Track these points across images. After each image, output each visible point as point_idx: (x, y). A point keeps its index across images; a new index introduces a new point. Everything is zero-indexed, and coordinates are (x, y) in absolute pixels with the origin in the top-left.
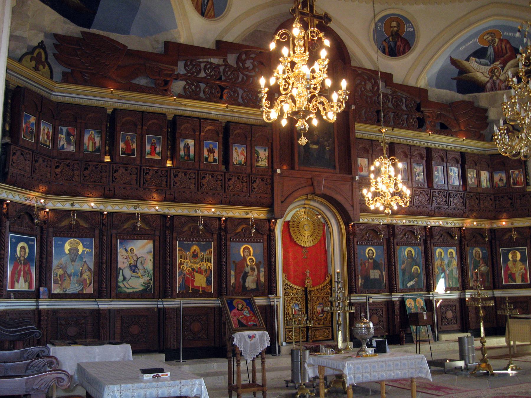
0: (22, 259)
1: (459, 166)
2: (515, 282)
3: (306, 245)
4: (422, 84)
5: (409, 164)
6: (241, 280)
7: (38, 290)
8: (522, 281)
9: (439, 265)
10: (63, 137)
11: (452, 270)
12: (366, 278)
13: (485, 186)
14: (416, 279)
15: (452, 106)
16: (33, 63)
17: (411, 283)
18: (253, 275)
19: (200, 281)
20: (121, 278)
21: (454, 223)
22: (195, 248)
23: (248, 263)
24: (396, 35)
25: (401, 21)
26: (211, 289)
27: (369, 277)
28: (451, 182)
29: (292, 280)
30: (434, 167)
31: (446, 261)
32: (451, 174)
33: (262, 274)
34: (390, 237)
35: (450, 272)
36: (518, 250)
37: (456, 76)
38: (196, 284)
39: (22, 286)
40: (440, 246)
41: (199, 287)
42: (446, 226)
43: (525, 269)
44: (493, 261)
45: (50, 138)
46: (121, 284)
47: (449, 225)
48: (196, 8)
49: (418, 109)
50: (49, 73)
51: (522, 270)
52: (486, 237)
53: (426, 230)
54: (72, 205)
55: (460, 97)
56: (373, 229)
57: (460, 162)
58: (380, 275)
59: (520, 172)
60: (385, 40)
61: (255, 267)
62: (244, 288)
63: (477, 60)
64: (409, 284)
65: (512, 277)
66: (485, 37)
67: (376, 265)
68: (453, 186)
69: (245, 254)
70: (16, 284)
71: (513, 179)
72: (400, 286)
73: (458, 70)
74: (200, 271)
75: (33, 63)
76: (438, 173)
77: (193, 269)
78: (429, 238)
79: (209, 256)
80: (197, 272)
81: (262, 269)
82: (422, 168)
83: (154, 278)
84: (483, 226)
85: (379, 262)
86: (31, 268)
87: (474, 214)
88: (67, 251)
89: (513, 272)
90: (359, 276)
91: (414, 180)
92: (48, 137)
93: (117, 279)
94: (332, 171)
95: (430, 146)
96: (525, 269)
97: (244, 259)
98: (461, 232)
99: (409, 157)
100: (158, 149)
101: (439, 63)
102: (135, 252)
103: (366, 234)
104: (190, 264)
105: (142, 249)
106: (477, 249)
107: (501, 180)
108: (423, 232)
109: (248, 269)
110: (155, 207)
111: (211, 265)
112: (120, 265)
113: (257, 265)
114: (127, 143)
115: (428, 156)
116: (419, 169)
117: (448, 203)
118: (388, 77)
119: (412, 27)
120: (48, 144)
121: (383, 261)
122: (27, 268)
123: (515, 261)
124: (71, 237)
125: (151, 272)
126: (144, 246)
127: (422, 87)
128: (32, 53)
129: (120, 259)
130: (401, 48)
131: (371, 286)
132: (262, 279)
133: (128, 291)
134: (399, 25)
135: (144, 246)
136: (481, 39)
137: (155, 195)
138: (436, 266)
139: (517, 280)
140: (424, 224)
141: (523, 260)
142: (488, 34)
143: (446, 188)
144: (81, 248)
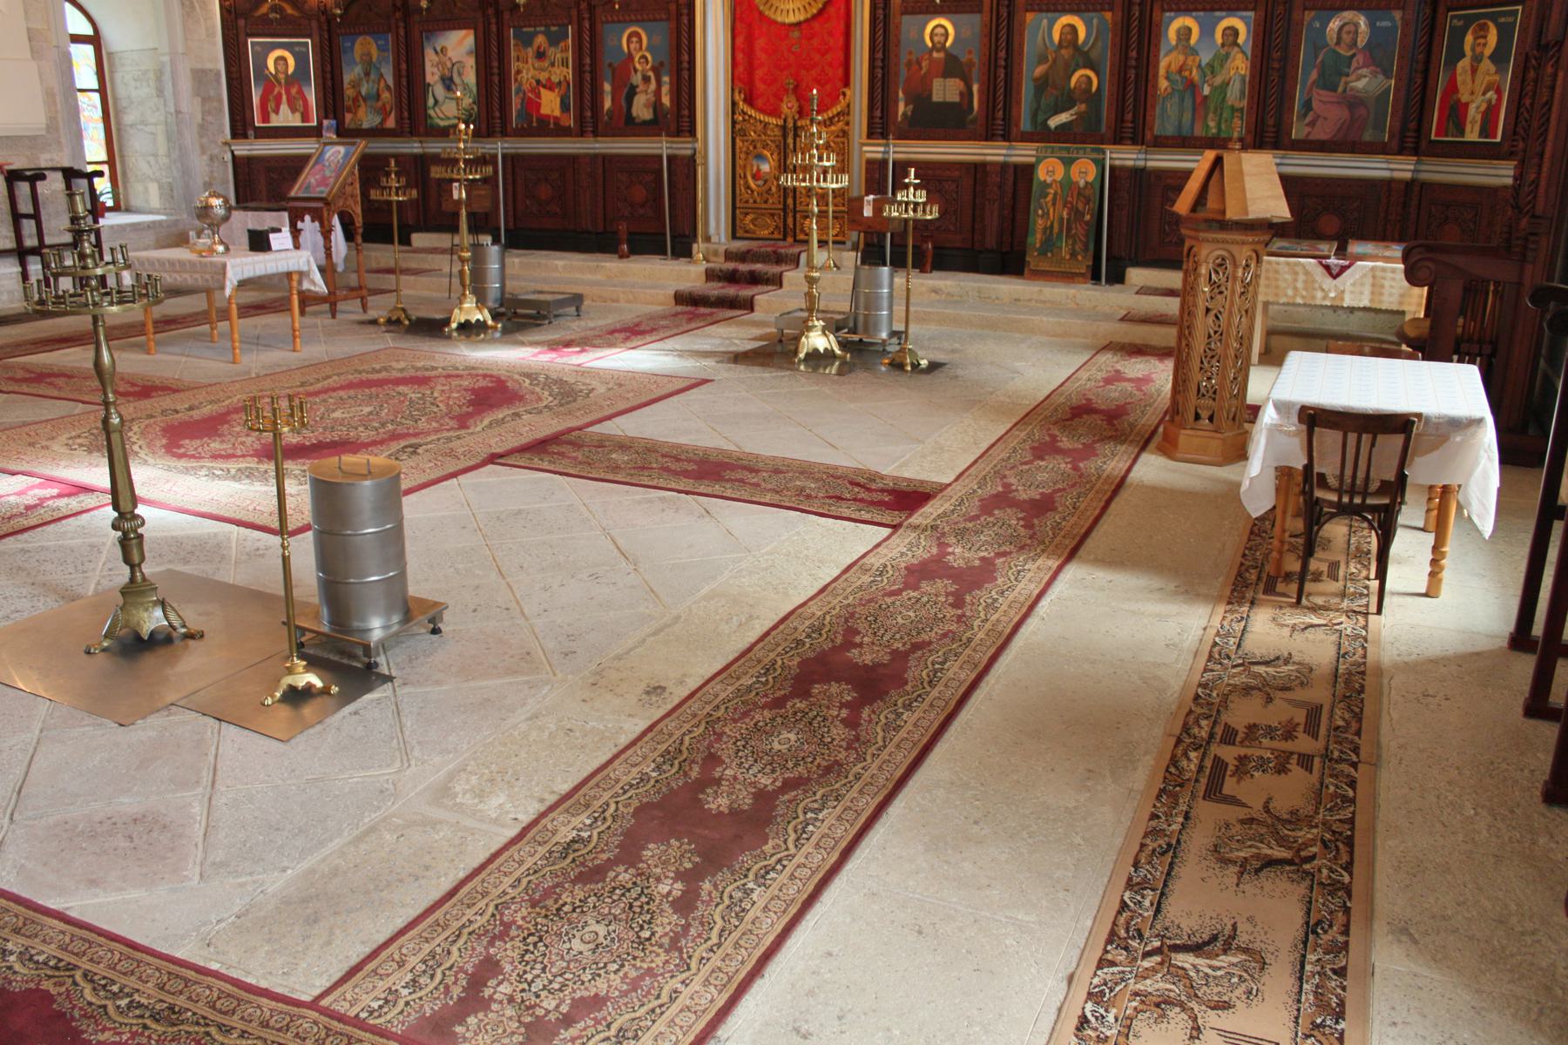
2: (1462, 134)
3: (791, 19)
6: (623, 103)
7: (320, 123)
8: (1483, 133)
9: (1174, 67)
12: (920, 99)
17: (1063, 118)
19: (550, 104)
20: (431, 102)
22: (540, 40)
29: (760, 102)
33: (665, 89)
38: (545, 110)
39: (285, 117)
41: (548, 116)
43: (1499, 92)
46: (431, 112)
51: (1489, 94)
58: (961, 94)
61: (651, 74)
62: (630, 119)
64: (1053, 122)
70: (273, 116)
72: (1025, 125)
74: (550, 86)
77: (538, 82)
80: (545, 87)
81: (666, 79)
83: (477, 102)
85: (964, 58)
88: (358, 59)
89: (1465, 98)
90: (901, 94)
96: (1499, 92)
97: (630, 57)
102: (450, 54)
104: (532, 72)
109: (637, 79)
112: (429, 79)
121: (974, 56)
122: (294, 91)
123: (1477, 59)
124: (360, 34)
125: (475, 89)
126: (461, 42)
129: (429, 68)
132: (666, 100)
133: (442, 124)
135: (461, 42)
138: (1162, 72)
139: (1468, 128)
141: (1499, 57)
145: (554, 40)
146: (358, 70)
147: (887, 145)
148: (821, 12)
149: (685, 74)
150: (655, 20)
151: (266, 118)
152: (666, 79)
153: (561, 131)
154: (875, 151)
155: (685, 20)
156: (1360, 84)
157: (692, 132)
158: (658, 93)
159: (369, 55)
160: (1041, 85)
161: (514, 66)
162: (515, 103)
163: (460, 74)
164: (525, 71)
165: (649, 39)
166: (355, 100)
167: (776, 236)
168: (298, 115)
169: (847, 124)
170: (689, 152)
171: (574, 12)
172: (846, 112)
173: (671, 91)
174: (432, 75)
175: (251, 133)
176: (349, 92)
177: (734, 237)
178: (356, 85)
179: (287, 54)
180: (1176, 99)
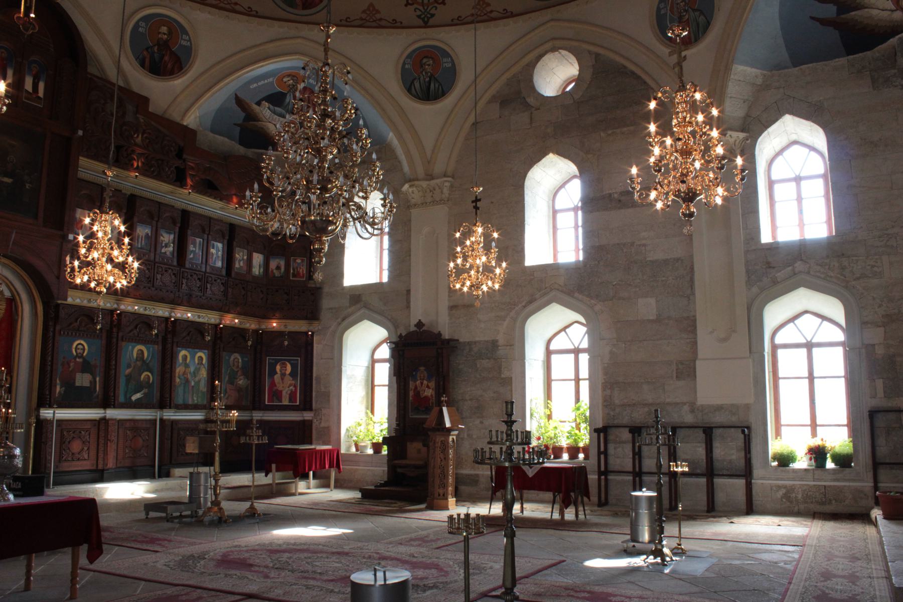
1: (226, 242)
4: (191, 120)
5: (154, 228)
8: (290, 401)
11: (199, 381)
12: (69, 384)
13: (257, 273)
14: (145, 390)
15: (226, 158)
17: (138, 396)
21: (209, 317)
24: (164, 46)
25: (176, 29)
27: (74, 383)
28: (210, 262)
30: (190, 239)
31: (192, 369)
32: (213, 251)
34: (113, 329)
35: (196, 383)
36: (289, 361)
37: (240, 122)
40: (185, 347)
42: (198, 320)
43: (295, 386)
44: (256, 373)
47: (201, 320)
49: (179, 155)
52: (98, 323)
53: (167, 324)
55: (241, 150)
56: (88, 315)
57: (227, 238)
58: (91, 382)
59: (303, 260)
60: (147, 49)
63: (271, 107)
64: (134, 398)
65: (277, 395)
66: (285, 80)
67: (86, 367)
68: (213, 268)
71: (294, 270)
72: (122, 399)
73: (243, 115)
76: (195, 247)
78: (173, 335)
82: (172, 236)
84: (247, 326)
87: (238, 309)
89: (280, 388)
91: (158, 252)
95: (190, 208)
96: (295, 386)
98: (216, 330)
99: (156, 219)
101: (218, 97)
103: (76, 321)
106: (237, 355)
107: (278, 268)
108: (163, 326)
115: (184, 223)
116: (167, 238)
117: (203, 289)
118: (144, 101)
119: (190, 40)
123: (283, 375)
127: (190, 126)
130: (169, 66)
131: (76, 398)
134: (170, 33)
136: (280, 80)
140: (167, 314)
141: (293, 374)
142: (289, 76)
143: (204, 270)
156: (240, 382)
160: (129, 378)
180: (182, 387)
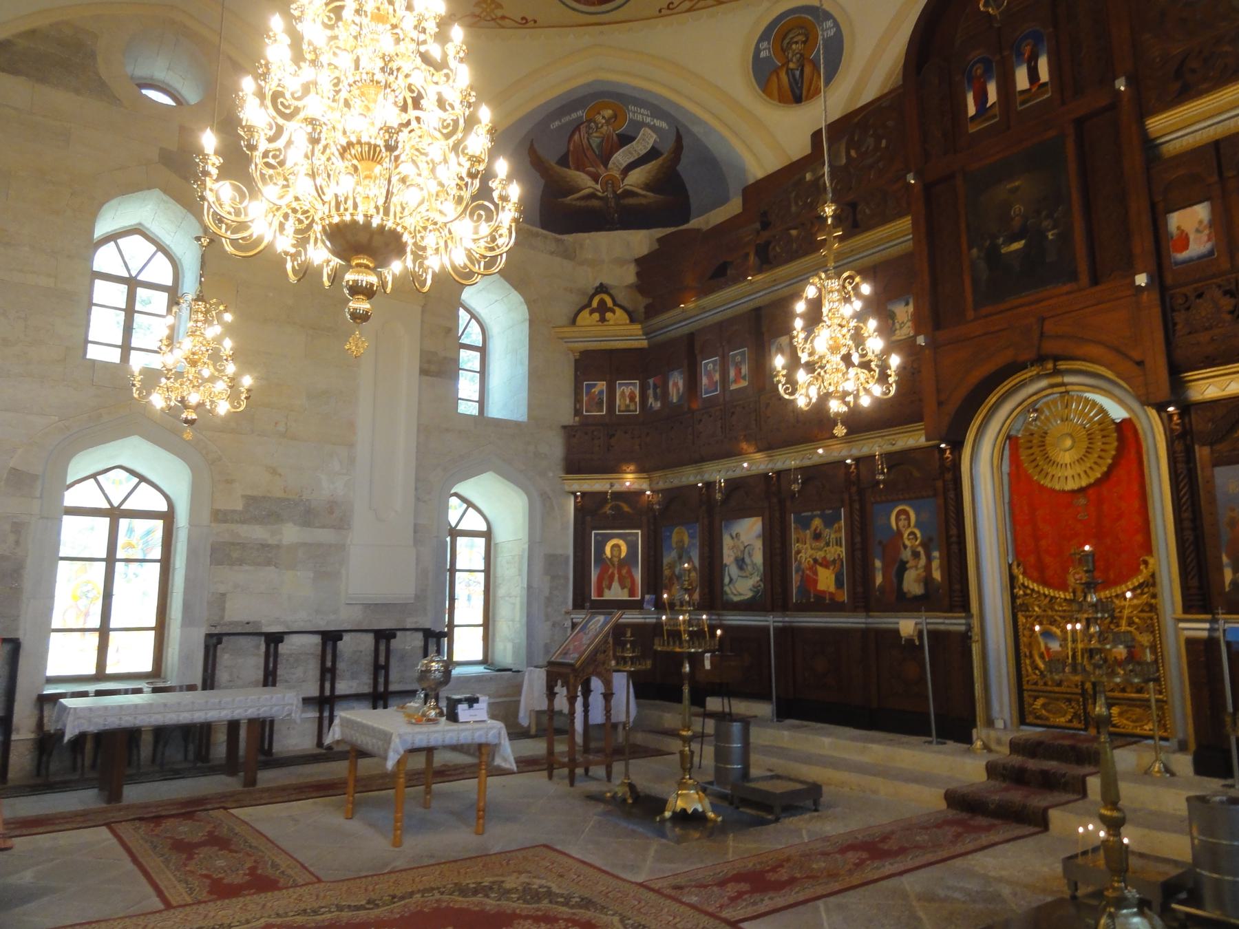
0: (616, 560)
3: (1071, 485)
6: (895, 580)
10: (651, 392)
16: (596, 316)
18: (916, 567)
19: (826, 580)
20: (727, 580)
22: (817, 522)
23: (907, 543)
26: (844, 597)
33: (935, 564)
38: (821, 586)
39: (616, 593)
41: (824, 592)
45: (637, 399)
48: (782, 99)
50: (626, 316)
54: (612, 485)
61: (920, 549)
69: (901, 524)
70: (606, 591)
74: (825, 564)
75: (596, 316)
77: (815, 561)
79: (838, 535)
80: (821, 565)
81: (936, 554)
86: (633, 570)
88: (674, 545)
90: (1225, 559)
92: (632, 398)
93: (722, 580)
94: (1067, 288)
97: (899, 534)
100: (745, 370)
102: (743, 538)
104: (810, 552)
105: (747, 534)
109: (906, 555)
110: (752, 463)
111: (842, 551)
113: (926, 544)
114: (710, 376)
120: (632, 407)
122: (624, 571)
128: (589, 304)
129: (726, 551)
132: (937, 575)
133: (736, 599)
137: (744, 446)
144: (686, 539)
145: (830, 522)
146: (674, 554)
147: (1214, 621)
148: (1107, 475)
149: (955, 548)
150: (923, 497)
151: (600, 593)
152: (936, 554)
153: (833, 606)
154: (1198, 628)
155: (952, 495)
157: (965, 607)
158: (928, 568)
159: (682, 541)
161: (794, 548)
162: (795, 580)
163: (750, 555)
164: (804, 551)
165: (917, 515)
166: (671, 579)
167: (1075, 724)
168: (626, 591)
169: (1154, 596)
170: (963, 628)
171: (846, 496)
172: (1152, 582)
173: (941, 566)
174: (728, 557)
175: (588, 604)
176: (667, 572)
177: (1022, 721)
178: (672, 566)
179: (621, 542)
